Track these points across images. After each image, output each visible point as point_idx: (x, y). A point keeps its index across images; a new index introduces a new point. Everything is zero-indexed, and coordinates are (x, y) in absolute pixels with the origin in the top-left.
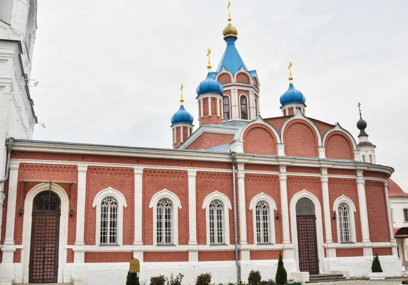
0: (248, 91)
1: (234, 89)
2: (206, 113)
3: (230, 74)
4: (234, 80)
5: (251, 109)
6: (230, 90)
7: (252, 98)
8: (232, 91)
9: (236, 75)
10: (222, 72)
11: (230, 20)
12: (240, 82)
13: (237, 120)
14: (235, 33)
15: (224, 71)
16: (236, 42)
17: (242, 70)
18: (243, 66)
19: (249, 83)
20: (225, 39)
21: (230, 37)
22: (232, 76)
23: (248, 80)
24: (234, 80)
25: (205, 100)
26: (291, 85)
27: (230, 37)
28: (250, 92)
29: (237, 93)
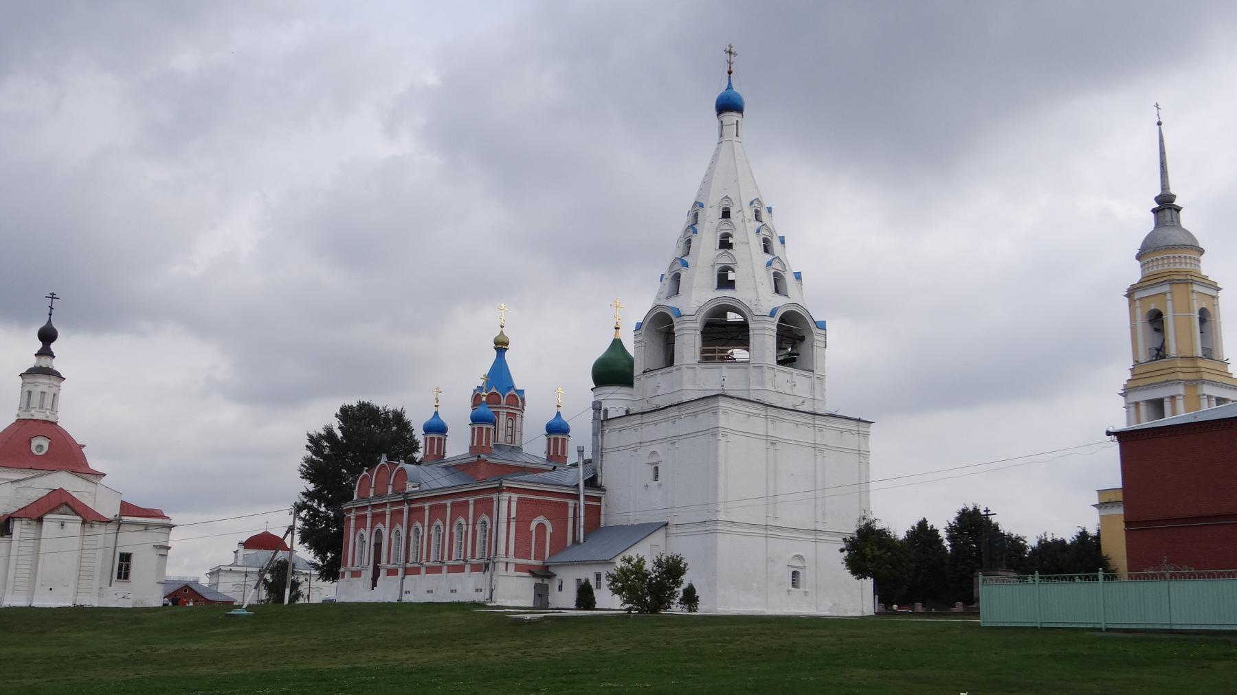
0: (515, 414)
2: (480, 441)
3: (501, 395)
6: (498, 412)
7: (518, 419)
11: (502, 327)
12: (509, 405)
14: (507, 344)
16: (507, 353)
17: (512, 392)
19: (518, 406)
20: (495, 349)
21: (501, 346)
22: (502, 398)
23: (516, 400)
24: (503, 401)
25: (481, 429)
26: (558, 413)
27: (501, 346)
29: (505, 417)
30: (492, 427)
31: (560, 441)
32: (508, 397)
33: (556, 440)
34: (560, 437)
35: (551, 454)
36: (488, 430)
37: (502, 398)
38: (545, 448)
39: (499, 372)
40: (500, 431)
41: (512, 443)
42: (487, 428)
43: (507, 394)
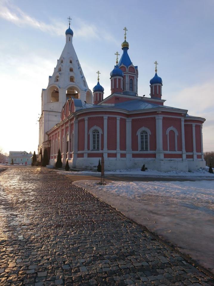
0: (134, 77)
1: (127, 75)
4: (127, 70)
5: (135, 86)
7: (135, 80)
8: (126, 76)
9: (128, 68)
10: (121, 66)
13: (128, 91)
15: (122, 65)
17: (131, 66)
18: (131, 63)
19: (134, 73)
22: (126, 68)
24: (127, 70)
27: (125, 47)
28: (135, 77)
29: (128, 77)
30: (121, 78)
31: (158, 87)
32: (130, 67)
33: (156, 87)
34: (158, 84)
35: (153, 93)
36: (120, 80)
37: (126, 68)
38: (150, 93)
39: (126, 59)
40: (126, 85)
41: (132, 91)
42: (119, 78)
43: (129, 67)
